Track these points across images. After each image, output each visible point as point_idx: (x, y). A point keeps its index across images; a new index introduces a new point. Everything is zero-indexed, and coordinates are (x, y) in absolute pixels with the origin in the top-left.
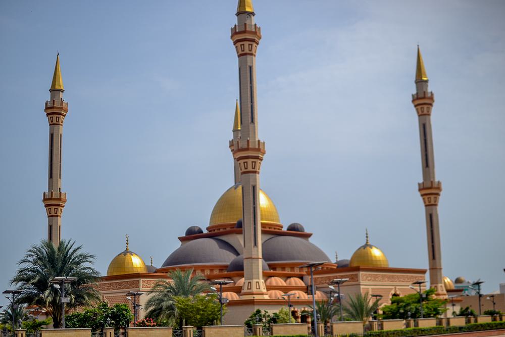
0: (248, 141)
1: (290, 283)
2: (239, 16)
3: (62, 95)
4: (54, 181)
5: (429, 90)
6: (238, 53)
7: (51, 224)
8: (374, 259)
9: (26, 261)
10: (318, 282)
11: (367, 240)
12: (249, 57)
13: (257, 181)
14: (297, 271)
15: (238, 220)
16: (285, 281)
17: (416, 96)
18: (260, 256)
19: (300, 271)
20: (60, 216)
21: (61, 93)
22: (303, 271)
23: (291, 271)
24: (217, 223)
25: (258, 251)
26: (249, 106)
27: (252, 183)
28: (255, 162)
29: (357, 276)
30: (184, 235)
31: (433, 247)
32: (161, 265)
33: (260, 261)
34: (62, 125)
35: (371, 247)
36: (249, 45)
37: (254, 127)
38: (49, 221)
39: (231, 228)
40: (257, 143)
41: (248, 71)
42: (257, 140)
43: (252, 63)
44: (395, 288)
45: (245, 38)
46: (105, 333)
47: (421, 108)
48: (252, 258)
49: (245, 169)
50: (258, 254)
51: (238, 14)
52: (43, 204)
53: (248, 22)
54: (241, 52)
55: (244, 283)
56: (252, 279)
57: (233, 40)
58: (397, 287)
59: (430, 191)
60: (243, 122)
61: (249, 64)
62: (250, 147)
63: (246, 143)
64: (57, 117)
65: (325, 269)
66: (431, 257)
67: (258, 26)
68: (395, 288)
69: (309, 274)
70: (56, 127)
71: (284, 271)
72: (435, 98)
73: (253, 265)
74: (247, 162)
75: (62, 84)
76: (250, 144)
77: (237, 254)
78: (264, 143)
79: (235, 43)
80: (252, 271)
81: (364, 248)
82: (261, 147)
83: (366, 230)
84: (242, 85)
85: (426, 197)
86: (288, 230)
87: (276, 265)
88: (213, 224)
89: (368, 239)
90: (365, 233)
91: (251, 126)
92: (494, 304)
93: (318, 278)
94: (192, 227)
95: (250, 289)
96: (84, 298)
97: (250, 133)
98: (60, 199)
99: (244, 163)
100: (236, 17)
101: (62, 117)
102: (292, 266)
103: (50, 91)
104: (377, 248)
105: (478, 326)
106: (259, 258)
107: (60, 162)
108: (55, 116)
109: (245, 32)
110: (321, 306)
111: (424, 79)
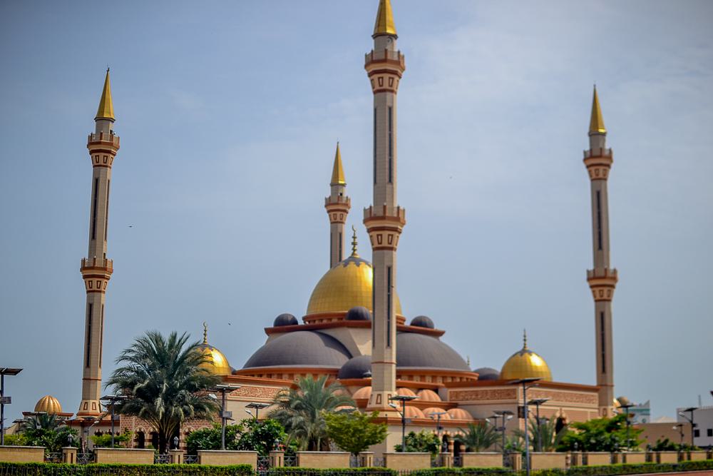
0: (385, 207)
1: (422, 395)
2: (377, 38)
3: (112, 126)
4: (97, 243)
5: (607, 147)
6: (373, 88)
7: (91, 302)
8: (534, 370)
9: (127, 359)
10: (461, 398)
11: (525, 344)
12: (389, 95)
13: (394, 260)
14: (428, 381)
15: (350, 309)
16: (416, 394)
17: (588, 154)
18: (394, 360)
19: (432, 382)
20: (104, 292)
21: (111, 123)
22: (436, 382)
23: (421, 381)
24: (319, 312)
25: (391, 354)
26: (387, 159)
27: (387, 264)
28: (392, 235)
29: (515, 391)
30: (272, 326)
31: (603, 356)
32: (243, 365)
33: (394, 366)
34: (110, 168)
35: (530, 353)
36: (390, 78)
37: (393, 188)
38: (88, 297)
39: (339, 319)
40: (396, 210)
41: (387, 114)
42: (396, 205)
43: (393, 102)
44: (561, 410)
45: (383, 68)
46: (273, 458)
47: (596, 170)
48: (383, 362)
49: (379, 243)
50: (391, 358)
51: (375, 36)
52: (81, 275)
53: (388, 47)
54: (377, 87)
55: (372, 395)
56: (383, 390)
57: (367, 71)
58: (563, 409)
59: (602, 281)
60: (378, 181)
61: (389, 104)
62: (387, 214)
63: (382, 210)
64: (104, 156)
65: (465, 380)
66: (601, 369)
67: (401, 54)
68: (561, 410)
69: (448, 386)
70: (103, 169)
71: (412, 380)
72: (614, 156)
73: (385, 372)
74: (381, 235)
75: (113, 110)
76: (387, 211)
77: (350, 356)
78: (404, 210)
79: (370, 75)
80: (383, 381)
81: (522, 355)
82: (401, 215)
83: (525, 331)
84: (378, 132)
85: (597, 290)
86: (412, 324)
87: (412, 373)
88: (313, 312)
89: (527, 342)
90: (523, 334)
91: (389, 186)
92: (683, 435)
93: (461, 392)
94: (283, 315)
95: (380, 403)
96: (205, 410)
97: (387, 196)
98: (105, 269)
99: (378, 235)
100: (373, 41)
101: (111, 156)
102: (423, 375)
103: (97, 119)
104: (538, 356)
105: (693, 464)
106: (392, 363)
107: (107, 218)
108: (102, 155)
109: (385, 61)
110: (476, 430)
111: (601, 131)
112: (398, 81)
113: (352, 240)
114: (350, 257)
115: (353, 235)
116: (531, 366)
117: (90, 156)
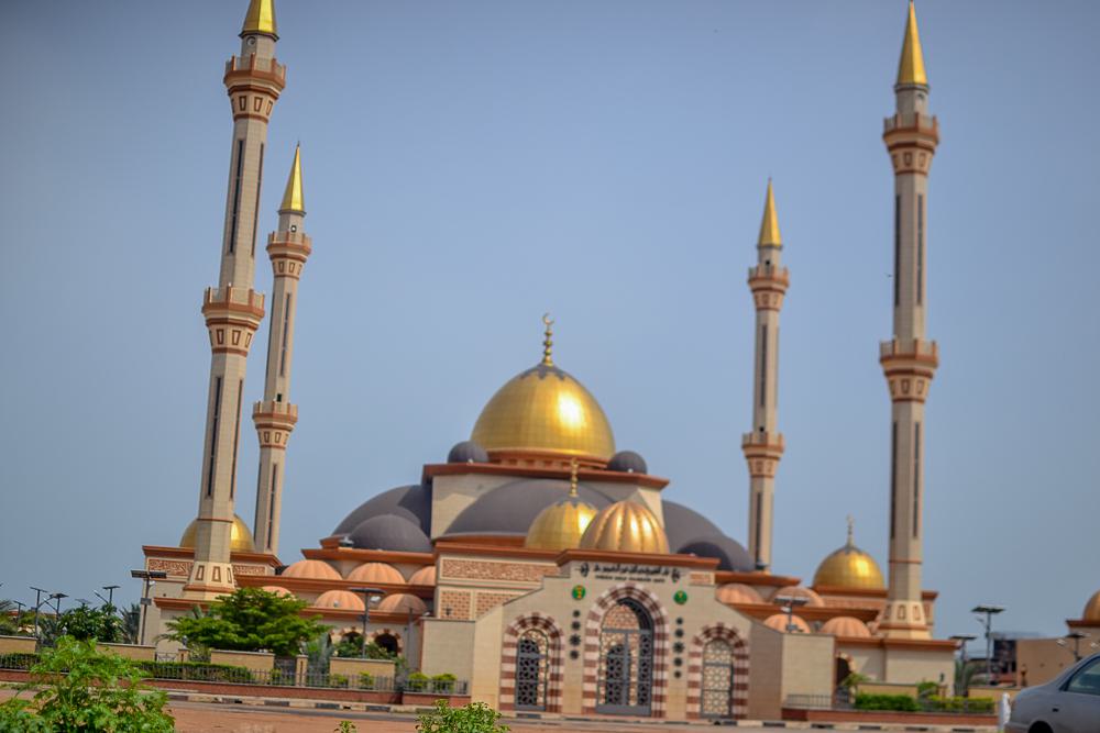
30: (444, 460)
52: (203, 319)
56: (893, 599)
89: (853, 536)
112: (931, 159)
113: (544, 338)
114: (540, 365)
115: (545, 330)
116: (845, 573)
117: (228, 99)
